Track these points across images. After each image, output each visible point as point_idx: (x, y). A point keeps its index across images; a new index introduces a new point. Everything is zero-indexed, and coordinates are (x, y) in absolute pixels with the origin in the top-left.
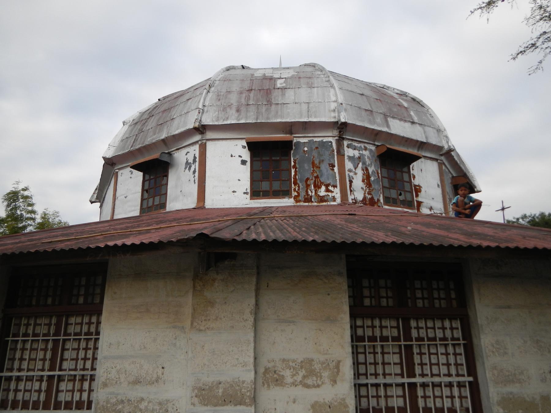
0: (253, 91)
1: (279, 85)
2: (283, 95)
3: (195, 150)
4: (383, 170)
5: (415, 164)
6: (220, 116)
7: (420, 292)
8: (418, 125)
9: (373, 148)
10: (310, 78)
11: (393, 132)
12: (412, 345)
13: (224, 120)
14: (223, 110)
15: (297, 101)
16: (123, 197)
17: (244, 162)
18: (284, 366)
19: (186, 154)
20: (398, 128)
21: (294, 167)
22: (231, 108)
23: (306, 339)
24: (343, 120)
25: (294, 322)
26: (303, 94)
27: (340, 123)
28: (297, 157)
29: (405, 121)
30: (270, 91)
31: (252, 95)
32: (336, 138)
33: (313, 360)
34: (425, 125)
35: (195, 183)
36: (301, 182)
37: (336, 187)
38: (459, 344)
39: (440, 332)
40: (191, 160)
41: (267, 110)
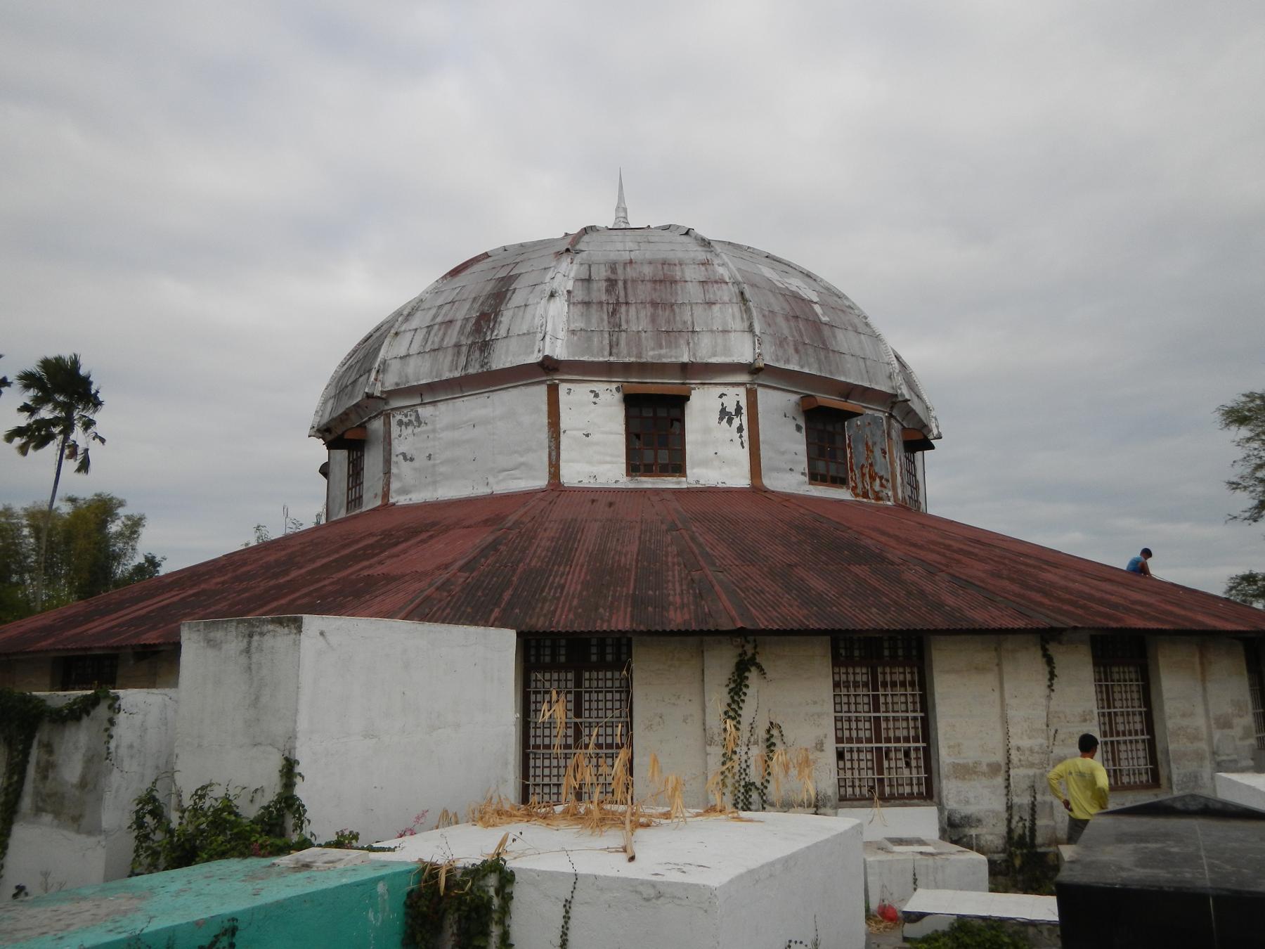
19: (721, 397)
40: (731, 408)
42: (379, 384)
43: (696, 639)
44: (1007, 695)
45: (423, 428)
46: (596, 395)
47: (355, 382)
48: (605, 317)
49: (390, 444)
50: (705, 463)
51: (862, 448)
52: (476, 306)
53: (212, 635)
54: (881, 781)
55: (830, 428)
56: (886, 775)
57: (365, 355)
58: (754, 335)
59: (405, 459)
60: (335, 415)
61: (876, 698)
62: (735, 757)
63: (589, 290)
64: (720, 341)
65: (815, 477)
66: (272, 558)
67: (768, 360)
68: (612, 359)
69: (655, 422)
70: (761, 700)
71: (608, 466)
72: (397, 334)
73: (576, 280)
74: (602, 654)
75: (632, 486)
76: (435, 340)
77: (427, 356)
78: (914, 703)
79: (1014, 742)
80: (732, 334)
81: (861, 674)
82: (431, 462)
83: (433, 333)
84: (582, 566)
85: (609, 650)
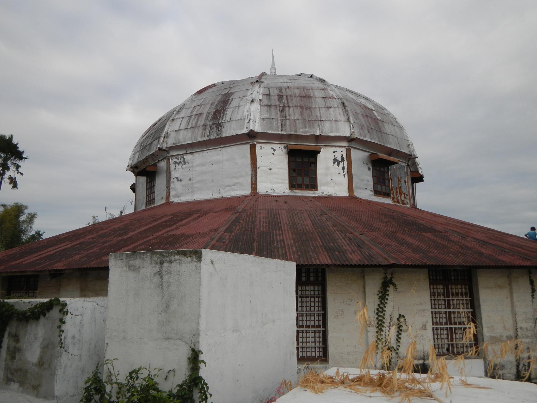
16: (266, 169)
19: (334, 152)
27: (413, 157)
40: (339, 158)
42: (165, 144)
43: (361, 270)
44: (515, 300)
45: (187, 165)
46: (274, 150)
47: (151, 143)
48: (279, 112)
49: (170, 173)
50: (326, 184)
51: (396, 180)
52: (213, 107)
53: (132, 262)
54: (452, 345)
55: (382, 169)
56: (454, 343)
57: (157, 130)
58: (350, 123)
59: (178, 180)
60: (140, 160)
61: (449, 301)
62: (382, 333)
63: (270, 100)
64: (334, 125)
65: (376, 193)
66: (116, 227)
67: (357, 135)
68: (283, 132)
69: (302, 163)
70: (395, 303)
71: (280, 185)
72: (173, 120)
73: (263, 95)
74: (308, 277)
75: (292, 194)
76: (193, 122)
77: (189, 130)
78: (467, 304)
79: (520, 325)
80: (340, 123)
81: (440, 289)
82: (191, 182)
83: (192, 119)
84: (288, 231)
85: (312, 275)
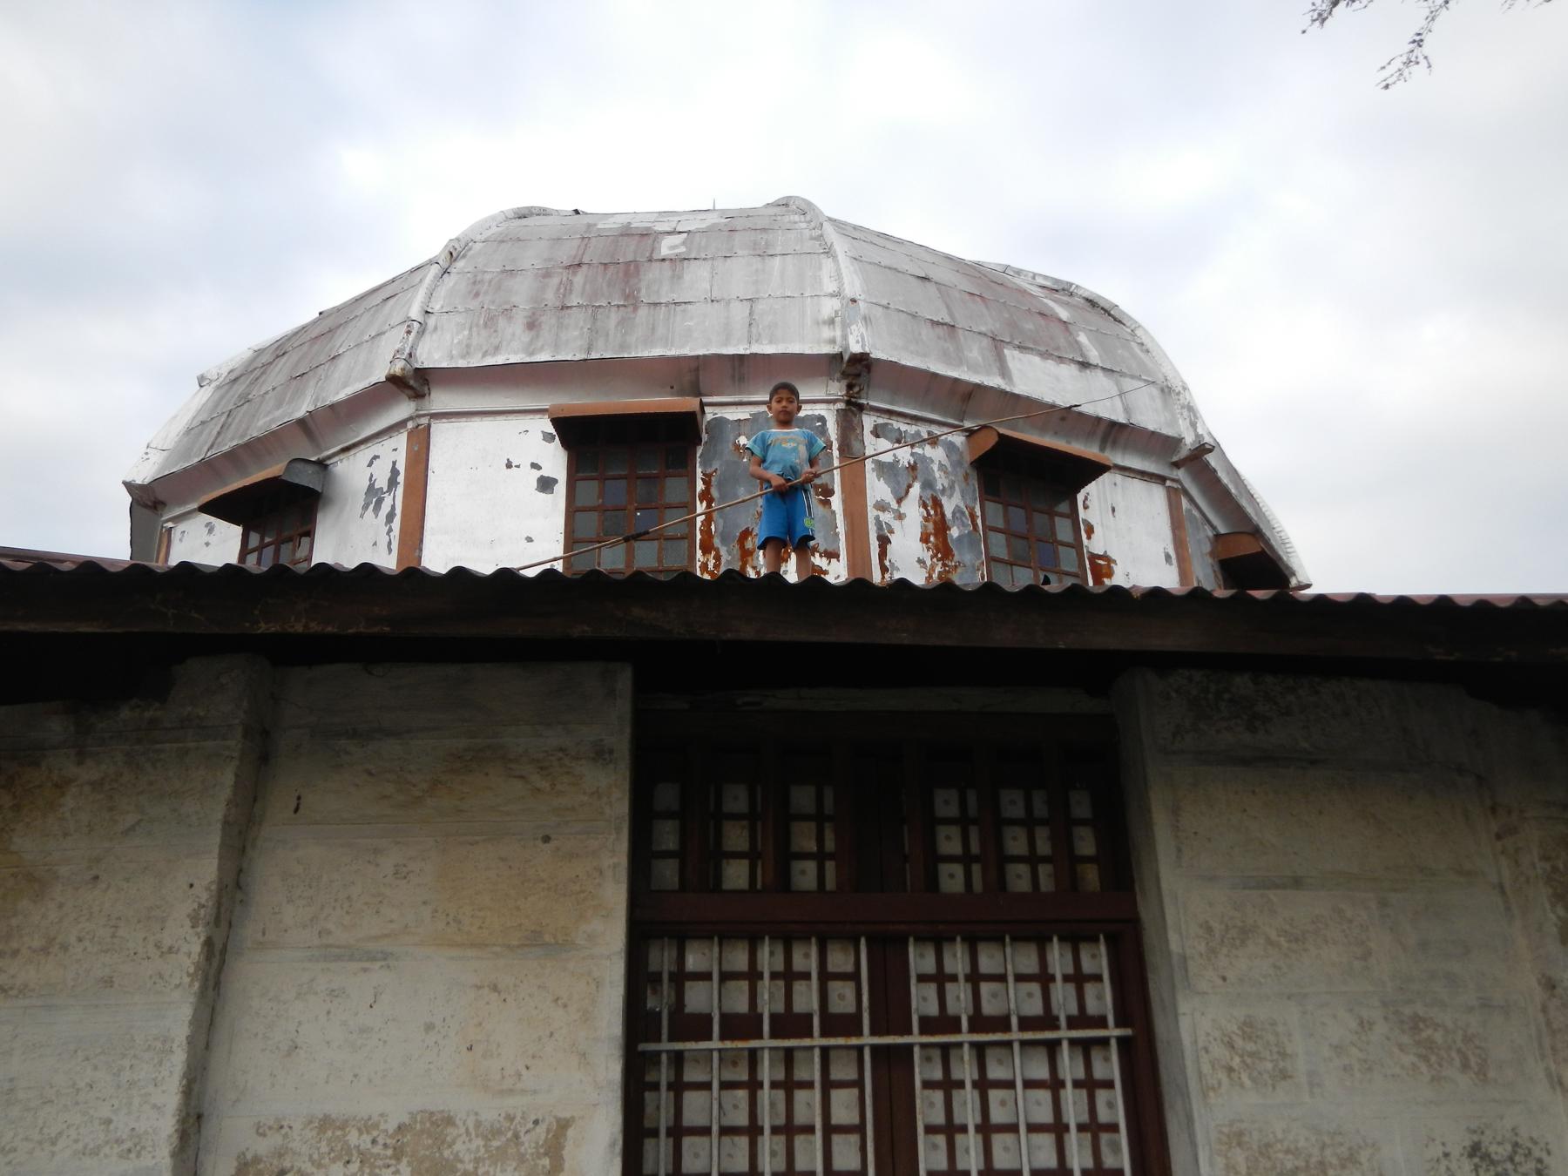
0: (584, 268)
1: (665, 251)
2: (677, 277)
3: (395, 451)
4: (990, 506)
5: (1092, 488)
6: (475, 342)
7: (954, 831)
8: (1100, 373)
9: (958, 439)
10: (764, 230)
11: (1020, 388)
12: (909, 1048)
13: (485, 355)
14: (486, 325)
15: (715, 295)
17: (546, 484)
18: (324, 1149)
19: (370, 465)
20: (1037, 378)
21: (706, 496)
22: (510, 318)
23: (429, 1027)
24: (856, 348)
25: (386, 956)
26: (738, 276)
27: (846, 357)
28: (716, 465)
29: (1061, 359)
30: (637, 268)
31: (579, 279)
32: (841, 406)
33: (449, 1121)
34: (1122, 374)
35: (390, 551)
36: (724, 541)
37: (837, 556)
38: (1104, 1042)
39: (1030, 995)
41: (621, 322)
